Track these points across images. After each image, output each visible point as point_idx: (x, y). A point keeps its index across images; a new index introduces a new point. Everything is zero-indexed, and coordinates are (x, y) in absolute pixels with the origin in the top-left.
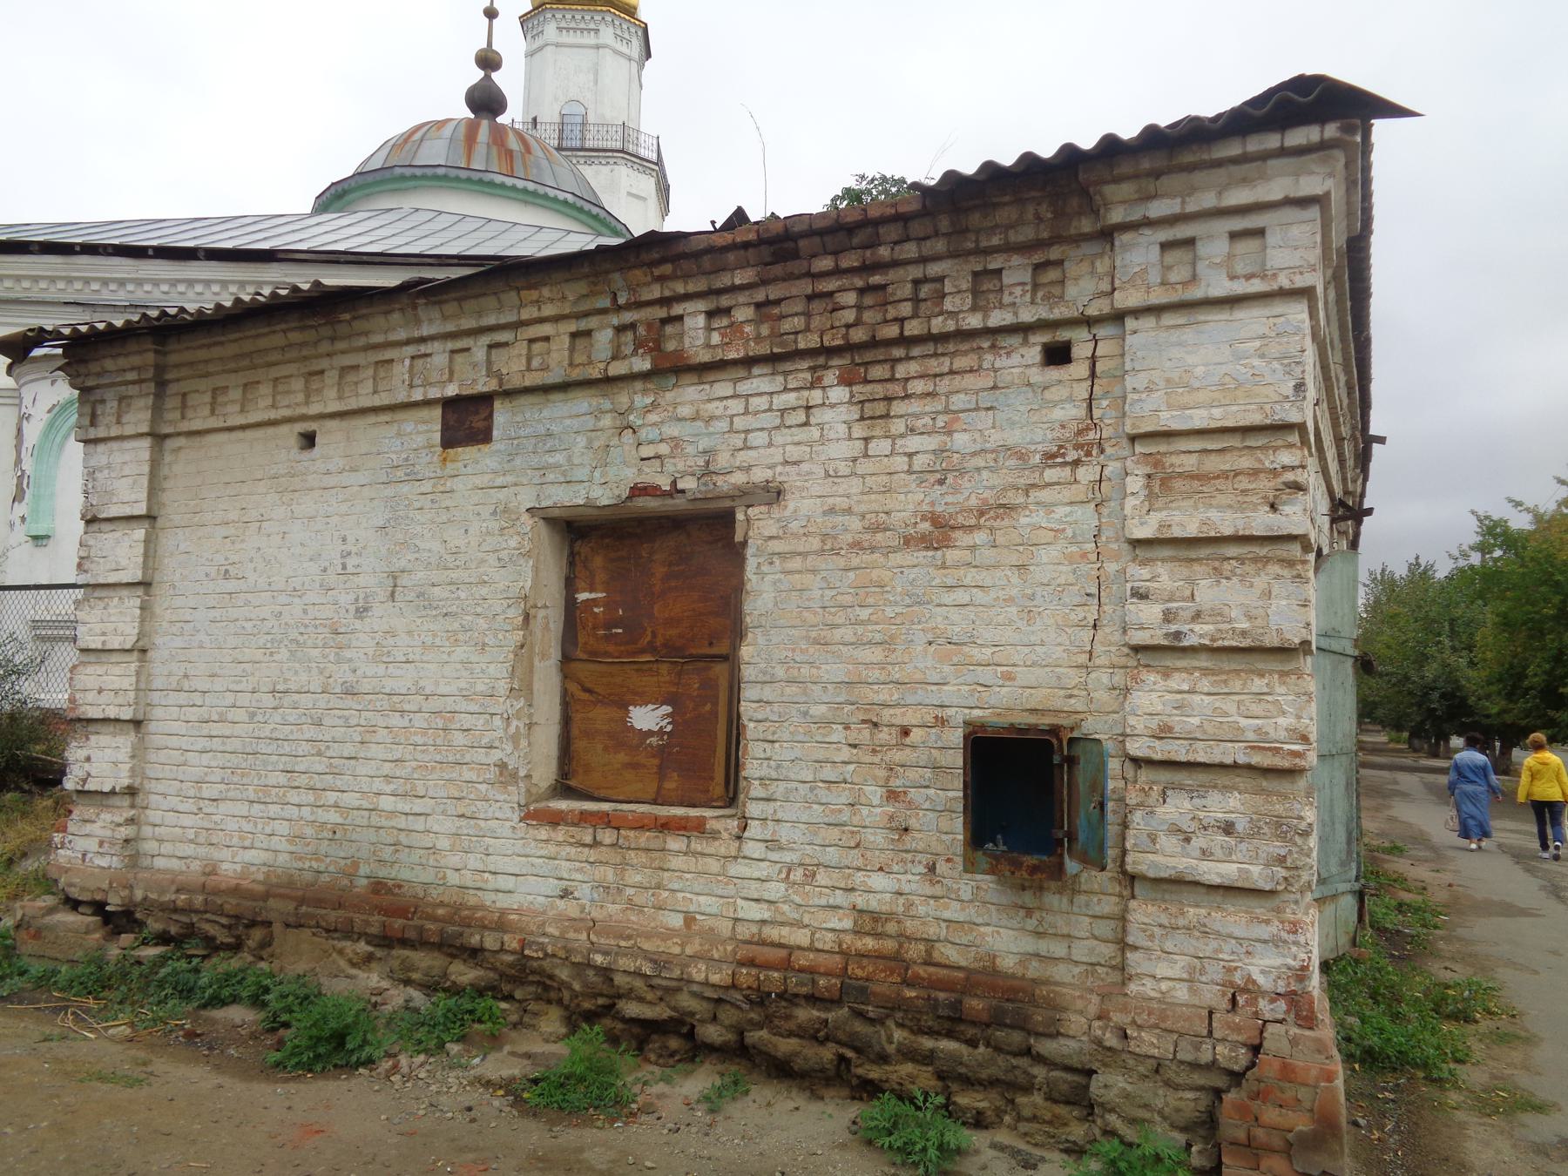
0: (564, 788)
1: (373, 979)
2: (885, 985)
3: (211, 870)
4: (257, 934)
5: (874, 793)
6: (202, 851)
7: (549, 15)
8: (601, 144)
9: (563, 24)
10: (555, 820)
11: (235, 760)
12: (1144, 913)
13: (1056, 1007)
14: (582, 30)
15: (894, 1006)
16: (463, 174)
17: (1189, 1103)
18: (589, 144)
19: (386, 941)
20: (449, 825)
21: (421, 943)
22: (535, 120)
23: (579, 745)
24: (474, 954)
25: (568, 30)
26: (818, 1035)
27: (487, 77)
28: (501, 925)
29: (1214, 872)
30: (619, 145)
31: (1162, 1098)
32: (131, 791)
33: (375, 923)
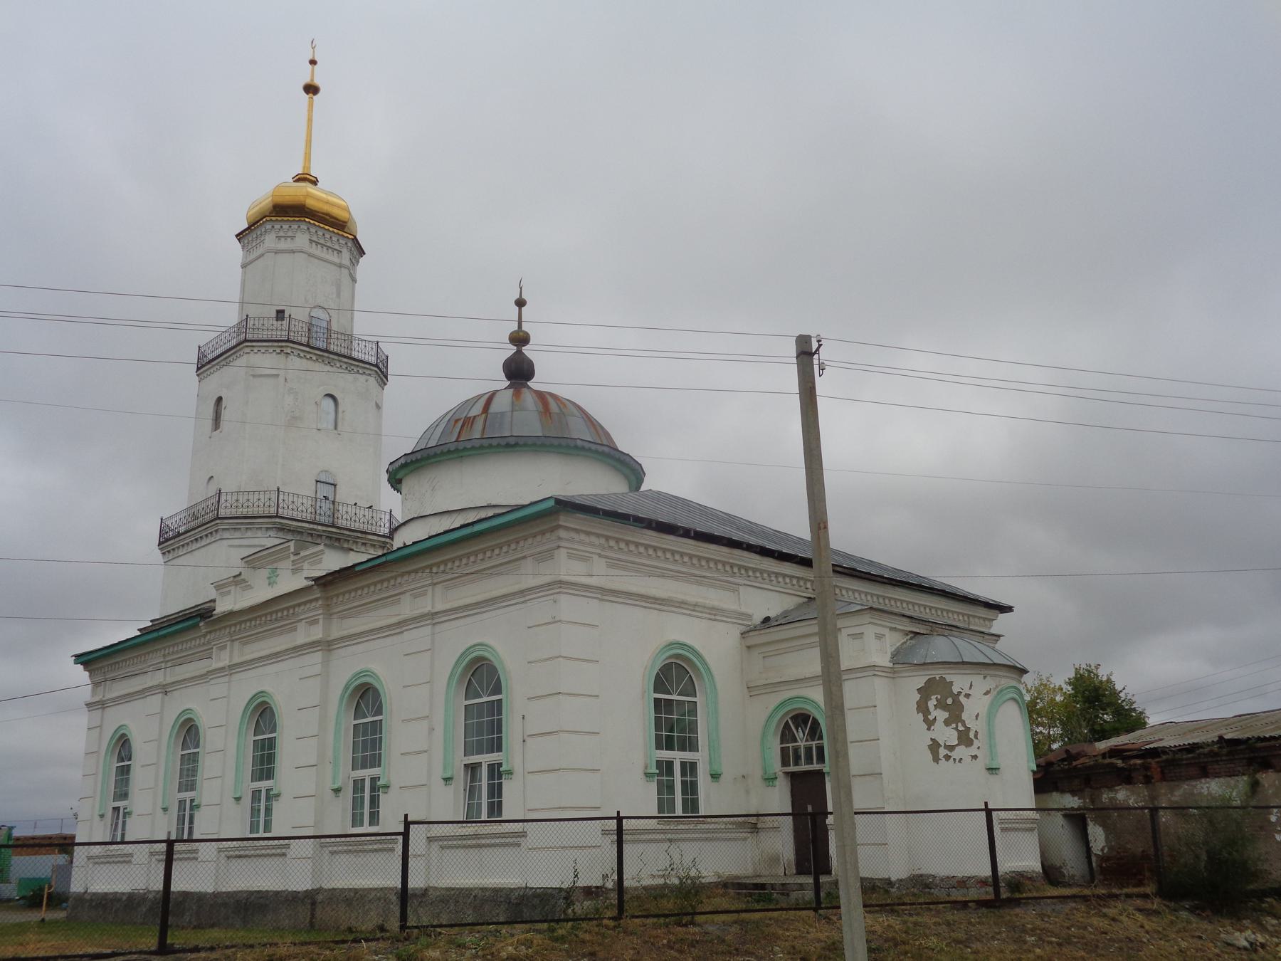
7: (304, 226)
9: (314, 238)
14: (328, 248)
18: (333, 348)
25: (317, 243)
27: (519, 352)
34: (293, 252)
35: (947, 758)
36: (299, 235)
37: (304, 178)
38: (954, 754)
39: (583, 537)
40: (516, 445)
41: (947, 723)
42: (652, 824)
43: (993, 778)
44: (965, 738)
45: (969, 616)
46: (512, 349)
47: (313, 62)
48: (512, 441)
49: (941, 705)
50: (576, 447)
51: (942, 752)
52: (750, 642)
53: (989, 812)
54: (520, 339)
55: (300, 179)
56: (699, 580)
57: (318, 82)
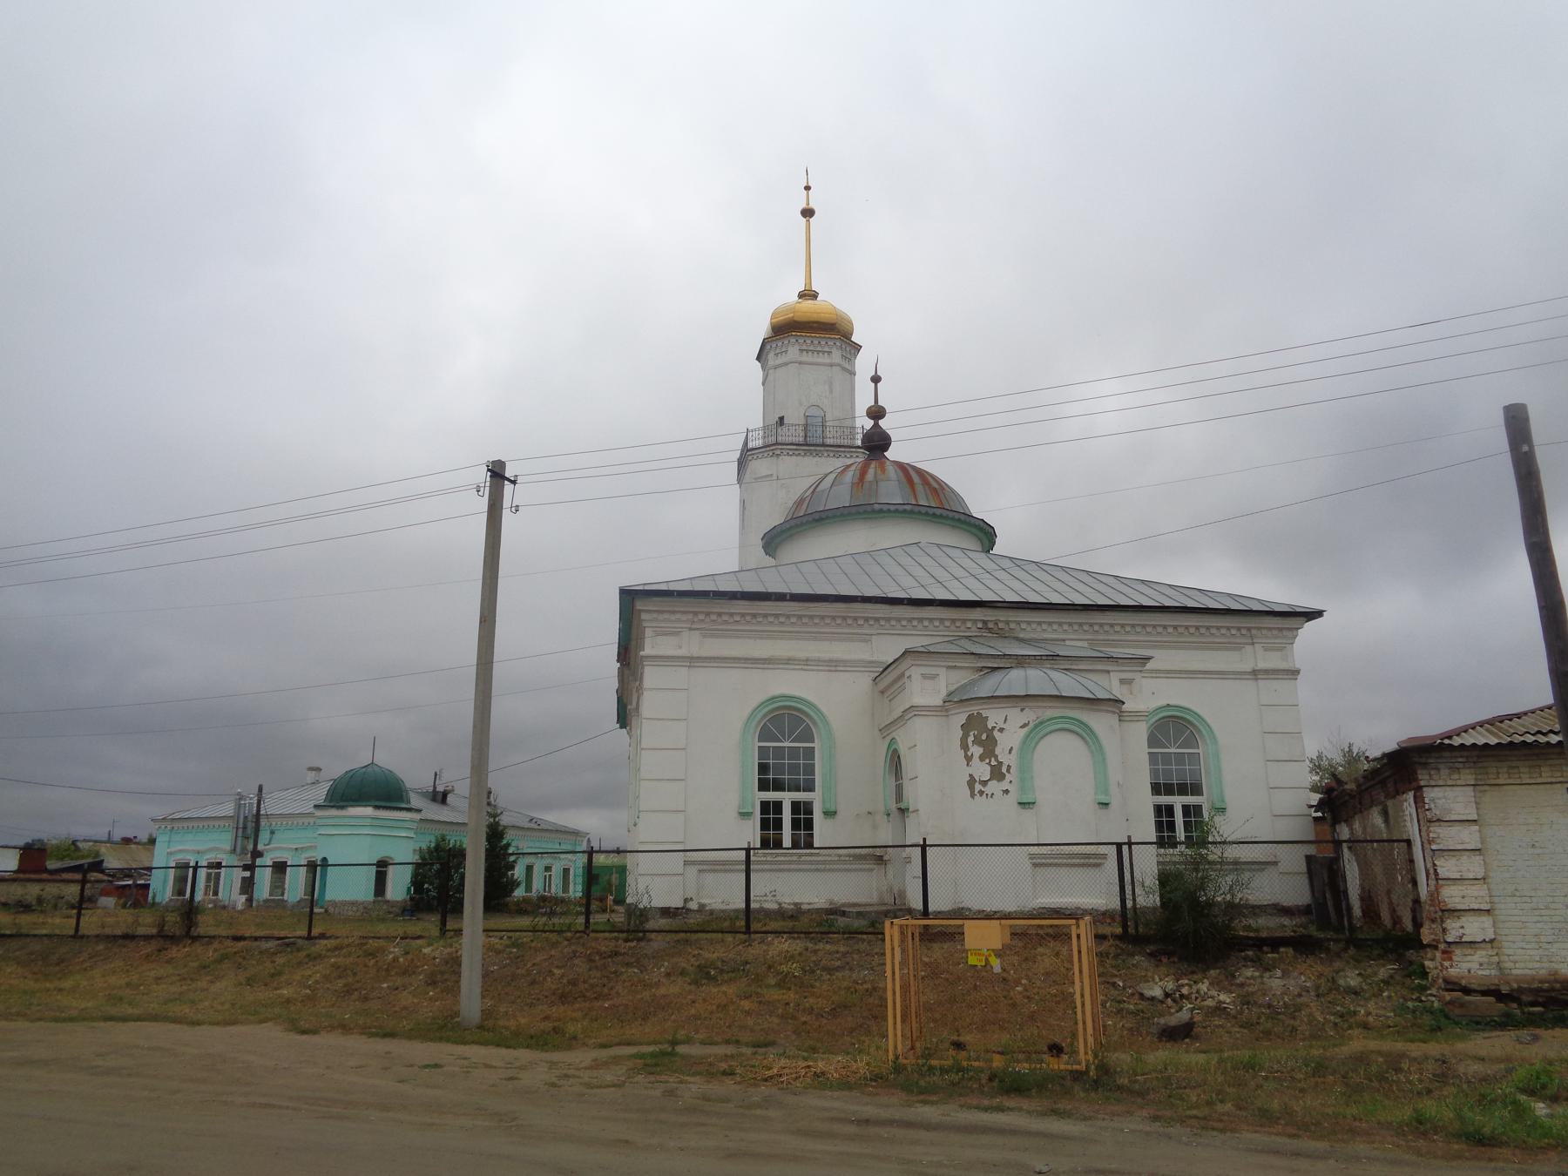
3: (1556, 973)
6: (1546, 965)
11: (1559, 926)
18: (828, 441)
22: (781, 419)
27: (876, 425)
32: (1492, 941)
34: (786, 364)
35: (981, 793)
36: (791, 349)
37: (808, 294)
38: (988, 790)
39: (666, 616)
40: (820, 520)
41: (982, 758)
43: (1027, 814)
44: (997, 773)
45: (1249, 629)
46: (872, 422)
48: (817, 516)
49: (977, 741)
50: (874, 511)
51: (978, 787)
52: (882, 686)
53: (924, 847)
54: (877, 413)
55: (802, 295)
57: (812, 205)
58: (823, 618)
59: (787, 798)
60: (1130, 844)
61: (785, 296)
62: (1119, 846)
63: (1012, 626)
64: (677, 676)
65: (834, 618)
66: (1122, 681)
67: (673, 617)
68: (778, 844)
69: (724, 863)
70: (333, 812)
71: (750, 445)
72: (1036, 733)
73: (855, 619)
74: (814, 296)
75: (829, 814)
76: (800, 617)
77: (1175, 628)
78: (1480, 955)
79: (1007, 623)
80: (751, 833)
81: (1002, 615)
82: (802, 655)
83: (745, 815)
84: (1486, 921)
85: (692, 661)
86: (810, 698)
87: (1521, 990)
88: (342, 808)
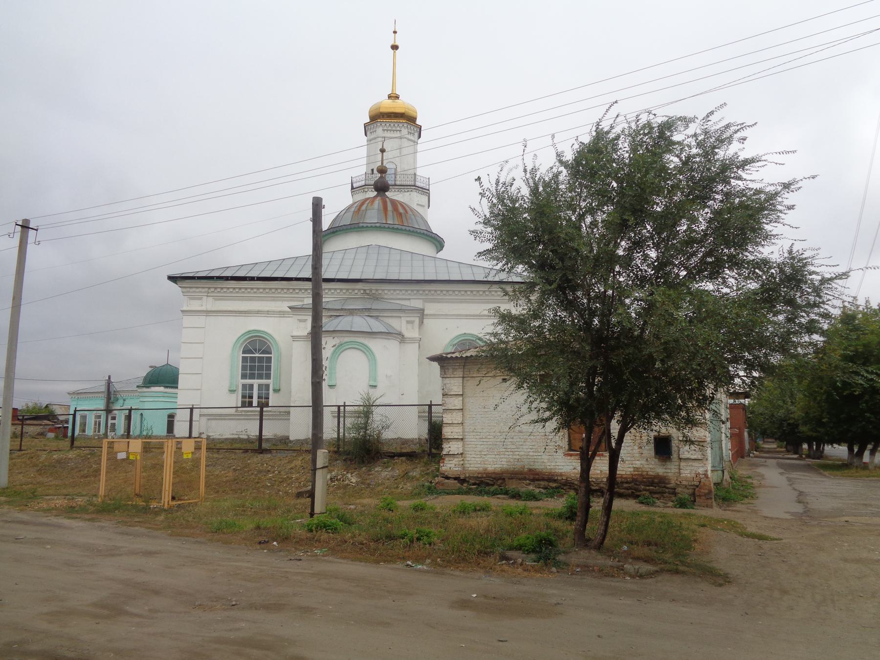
0: (570, 449)
1: (531, 487)
2: (640, 479)
4: (500, 481)
5: (636, 448)
8: (405, 183)
10: (571, 455)
12: (683, 464)
13: (669, 479)
15: (642, 482)
16: (383, 225)
17: (691, 491)
18: (398, 183)
19: (533, 480)
20: (547, 457)
21: (543, 480)
23: (573, 441)
24: (555, 481)
26: (627, 489)
28: (561, 475)
29: (693, 457)
30: (413, 183)
31: (686, 491)
32: (462, 454)
33: (531, 477)
37: (394, 97)
39: (194, 289)
42: (233, 411)
47: (395, 32)
50: (359, 227)
56: (274, 299)
58: (277, 289)
59: (256, 382)
60: (344, 406)
61: (379, 99)
62: (339, 407)
63: (380, 292)
64: (200, 320)
65: (282, 289)
66: (408, 322)
67: (198, 290)
68: (250, 404)
69: (221, 415)
70: (145, 390)
71: (355, 185)
72: (339, 349)
73: (294, 289)
74: (397, 97)
75: (277, 391)
76: (264, 289)
77: (472, 291)
78: (455, 461)
79: (377, 290)
80: (235, 400)
81: (374, 287)
82: (266, 309)
83: (232, 391)
84: (460, 444)
85: (208, 313)
86: (270, 332)
87: (470, 477)
88: (148, 387)
